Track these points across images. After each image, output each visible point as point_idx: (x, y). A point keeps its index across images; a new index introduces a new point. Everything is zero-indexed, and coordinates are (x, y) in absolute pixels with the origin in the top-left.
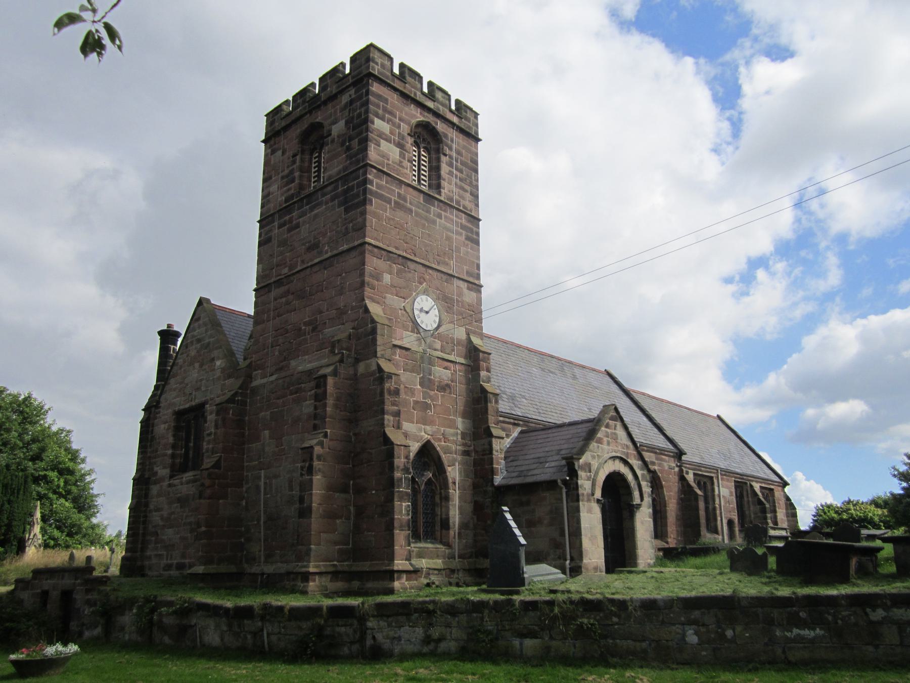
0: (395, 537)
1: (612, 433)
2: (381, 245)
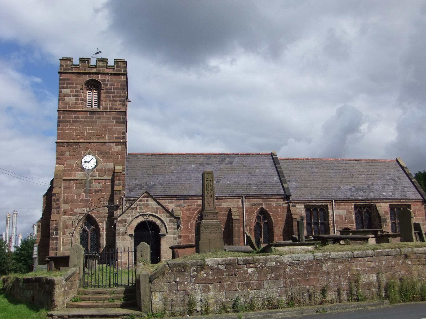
0: (50, 254)
1: (143, 204)
2: (65, 141)
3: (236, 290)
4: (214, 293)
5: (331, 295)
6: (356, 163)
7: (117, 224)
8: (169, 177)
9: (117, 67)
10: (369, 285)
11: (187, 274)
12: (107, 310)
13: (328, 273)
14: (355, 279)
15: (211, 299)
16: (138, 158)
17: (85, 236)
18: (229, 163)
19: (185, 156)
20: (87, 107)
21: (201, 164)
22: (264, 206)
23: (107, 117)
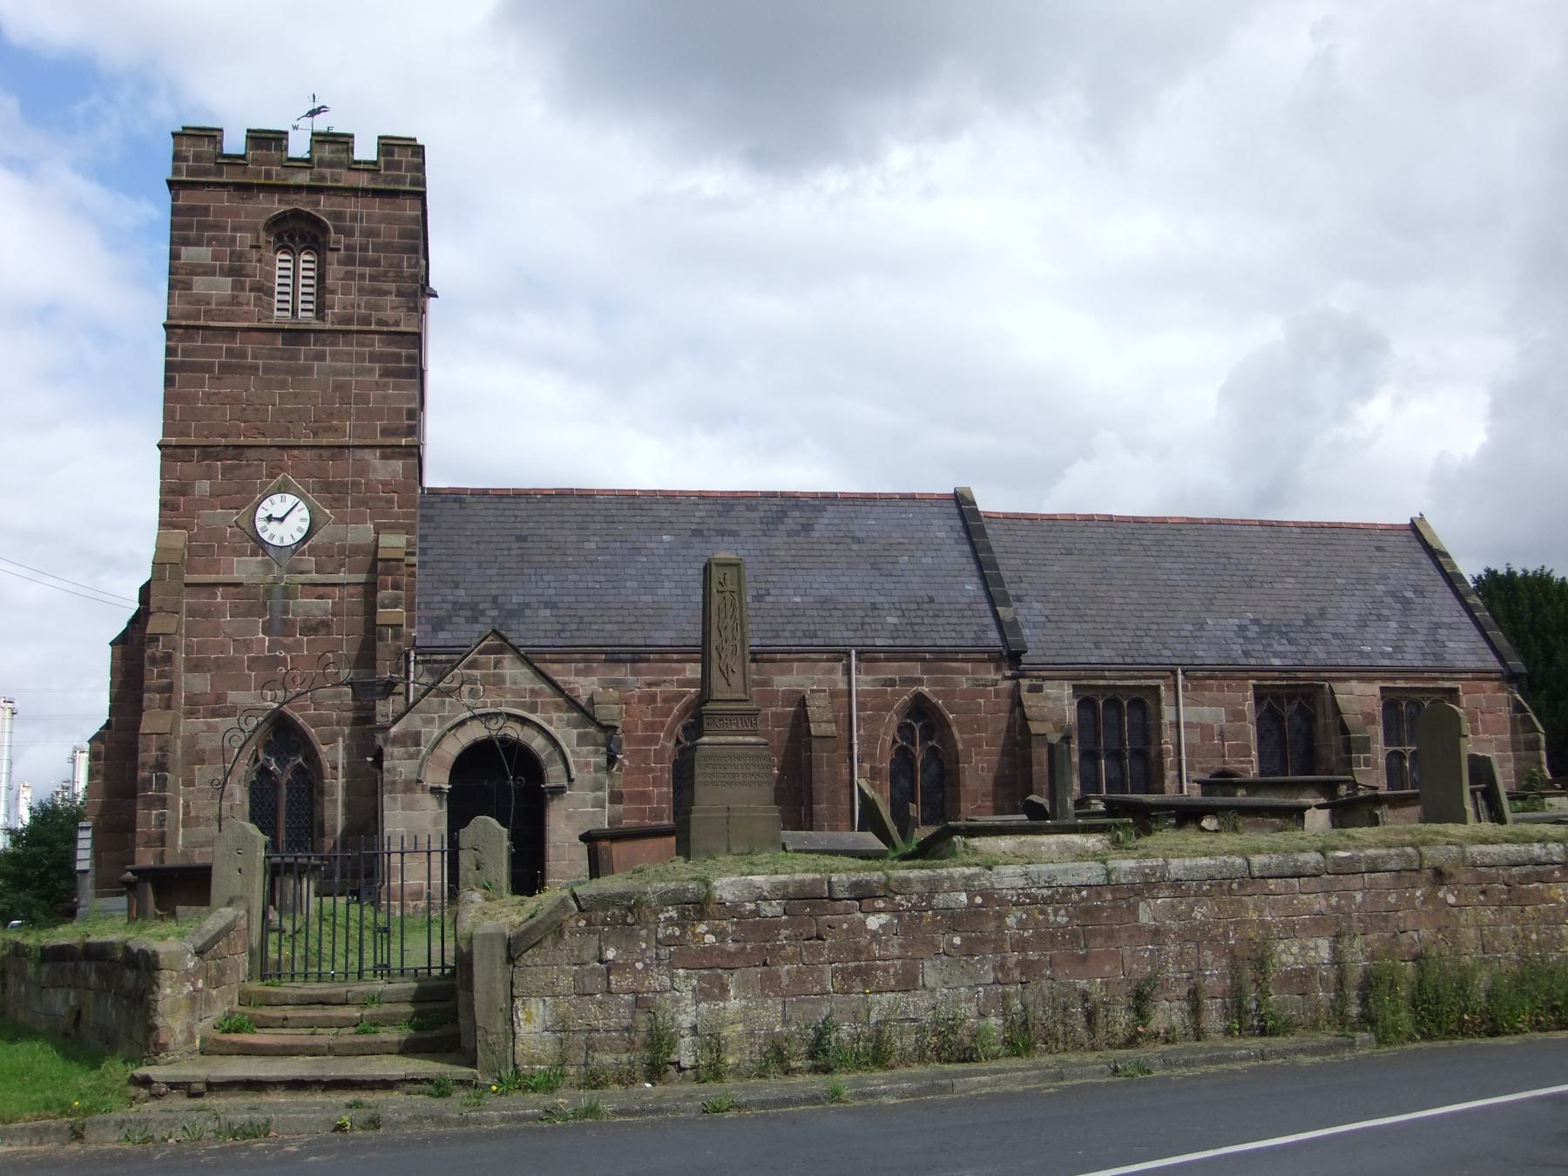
1: (484, 676)
2: (192, 440)
3: (824, 993)
4: (744, 1002)
5: (1167, 1014)
6: (1266, 535)
7: (385, 749)
8: (578, 578)
9: (389, 166)
10: (1302, 979)
11: (644, 932)
12: (352, 1061)
13: (1157, 934)
14: (1252, 955)
15: (733, 1023)
16: (463, 505)
17: (267, 792)
18: (800, 528)
19: (636, 500)
20: (276, 313)
21: (697, 533)
22: (927, 690)
23: (349, 354)
